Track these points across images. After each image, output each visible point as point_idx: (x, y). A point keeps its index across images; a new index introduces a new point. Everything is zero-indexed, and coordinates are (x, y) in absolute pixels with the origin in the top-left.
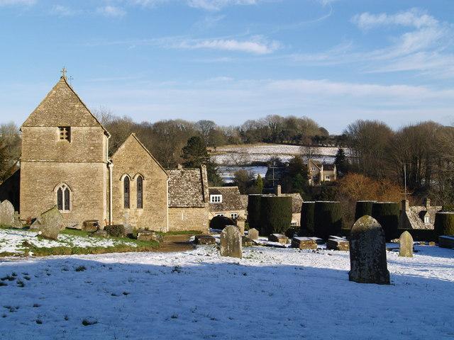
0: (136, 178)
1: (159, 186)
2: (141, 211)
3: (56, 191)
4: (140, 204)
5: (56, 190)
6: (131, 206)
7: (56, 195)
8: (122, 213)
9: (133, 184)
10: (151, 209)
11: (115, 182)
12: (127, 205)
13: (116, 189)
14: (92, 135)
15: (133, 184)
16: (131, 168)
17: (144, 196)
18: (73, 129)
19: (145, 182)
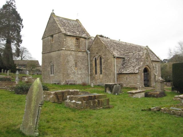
0: (99, 58)
1: (109, 61)
2: (101, 76)
3: (50, 66)
4: (101, 73)
5: (50, 65)
6: (97, 73)
7: (50, 67)
8: (94, 77)
9: (98, 62)
10: (106, 75)
11: (91, 61)
12: (96, 73)
13: (91, 65)
14: (59, 37)
15: (98, 62)
16: (97, 53)
17: (103, 68)
18: (54, 36)
19: (103, 60)
